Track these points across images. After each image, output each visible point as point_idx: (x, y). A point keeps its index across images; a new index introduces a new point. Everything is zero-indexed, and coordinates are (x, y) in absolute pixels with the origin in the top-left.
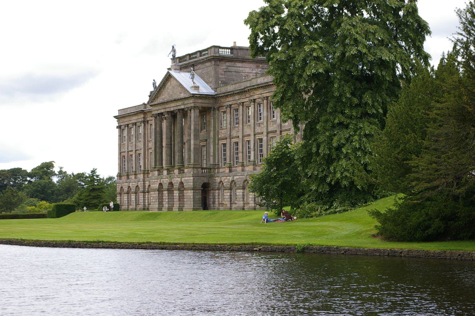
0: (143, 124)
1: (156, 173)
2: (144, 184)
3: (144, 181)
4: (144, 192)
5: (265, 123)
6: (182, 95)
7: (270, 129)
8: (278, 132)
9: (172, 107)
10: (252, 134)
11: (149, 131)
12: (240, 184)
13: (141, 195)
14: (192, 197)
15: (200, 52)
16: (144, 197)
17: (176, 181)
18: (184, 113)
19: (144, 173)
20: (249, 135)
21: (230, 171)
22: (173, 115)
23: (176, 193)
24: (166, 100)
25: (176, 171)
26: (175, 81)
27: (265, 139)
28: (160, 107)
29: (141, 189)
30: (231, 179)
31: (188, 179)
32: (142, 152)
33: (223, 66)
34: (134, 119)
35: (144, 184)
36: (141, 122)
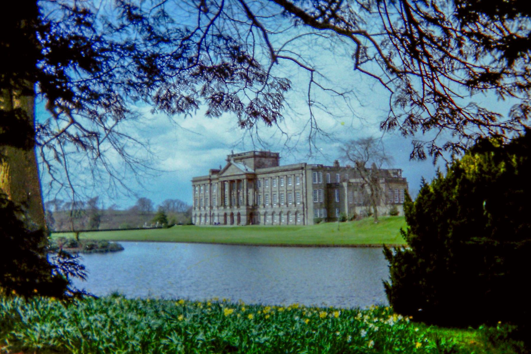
1: (222, 208)
4: (210, 216)
6: (239, 173)
8: (293, 190)
10: (285, 190)
12: (277, 212)
13: (208, 218)
15: (245, 153)
17: (236, 211)
18: (239, 181)
20: (276, 191)
21: (264, 207)
22: (232, 182)
23: (236, 218)
24: (229, 174)
25: (236, 207)
29: (209, 214)
31: (243, 210)
32: (209, 198)
33: (257, 159)
34: (203, 182)
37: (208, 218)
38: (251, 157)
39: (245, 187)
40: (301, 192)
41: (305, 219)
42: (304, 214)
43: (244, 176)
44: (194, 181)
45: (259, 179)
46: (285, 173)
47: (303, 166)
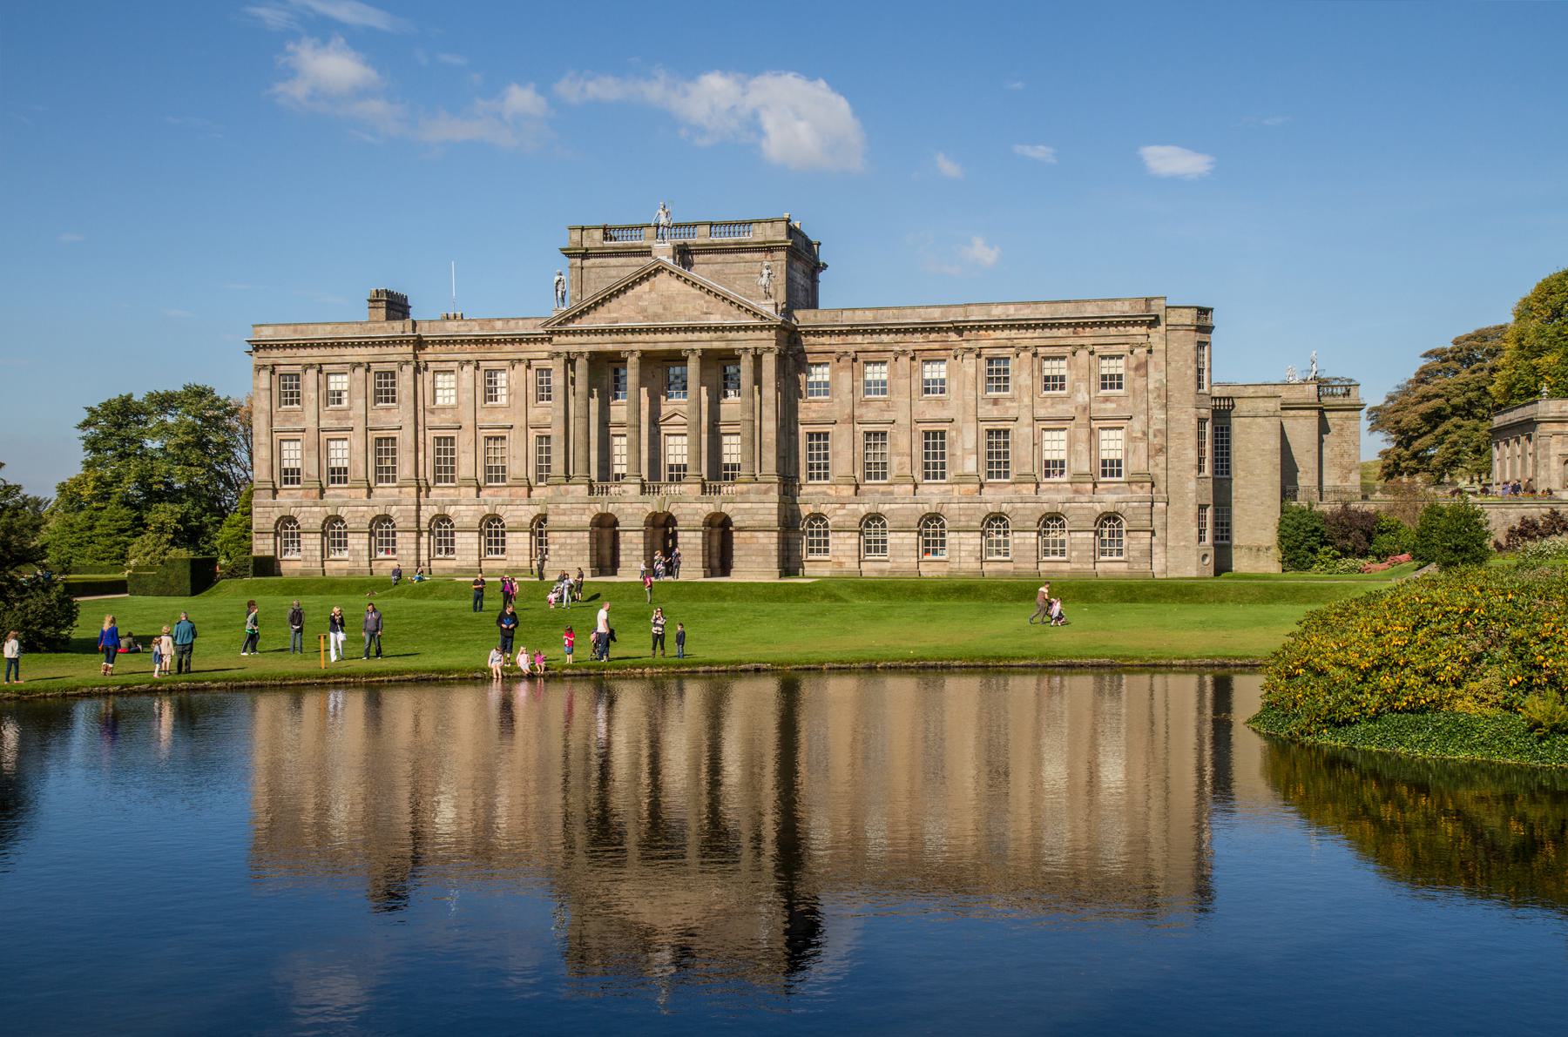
0: (409, 370)
2: (418, 510)
3: (419, 505)
4: (419, 533)
5: (1027, 400)
6: (715, 320)
7: (1041, 413)
8: (1082, 419)
9: (664, 342)
11: (428, 386)
14: (774, 547)
16: (418, 543)
17: (691, 507)
19: (419, 489)
26: (677, 285)
27: (1021, 433)
28: (598, 338)
30: (863, 509)
32: (405, 438)
35: (418, 510)
36: (401, 364)
37: (405, 542)
38: (768, 248)
39: (770, 391)
40: (1137, 426)
41: (1157, 550)
42: (1153, 533)
43: (767, 339)
44: (258, 346)
45: (810, 359)
46: (1027, 337)
47: (1157, 308)
